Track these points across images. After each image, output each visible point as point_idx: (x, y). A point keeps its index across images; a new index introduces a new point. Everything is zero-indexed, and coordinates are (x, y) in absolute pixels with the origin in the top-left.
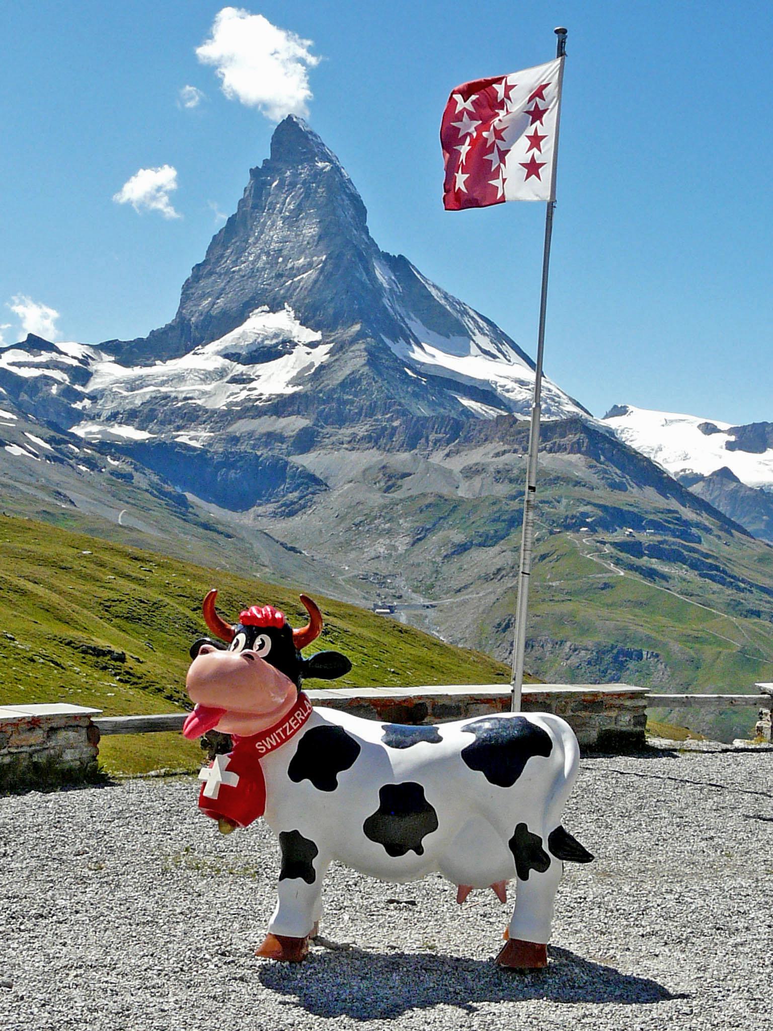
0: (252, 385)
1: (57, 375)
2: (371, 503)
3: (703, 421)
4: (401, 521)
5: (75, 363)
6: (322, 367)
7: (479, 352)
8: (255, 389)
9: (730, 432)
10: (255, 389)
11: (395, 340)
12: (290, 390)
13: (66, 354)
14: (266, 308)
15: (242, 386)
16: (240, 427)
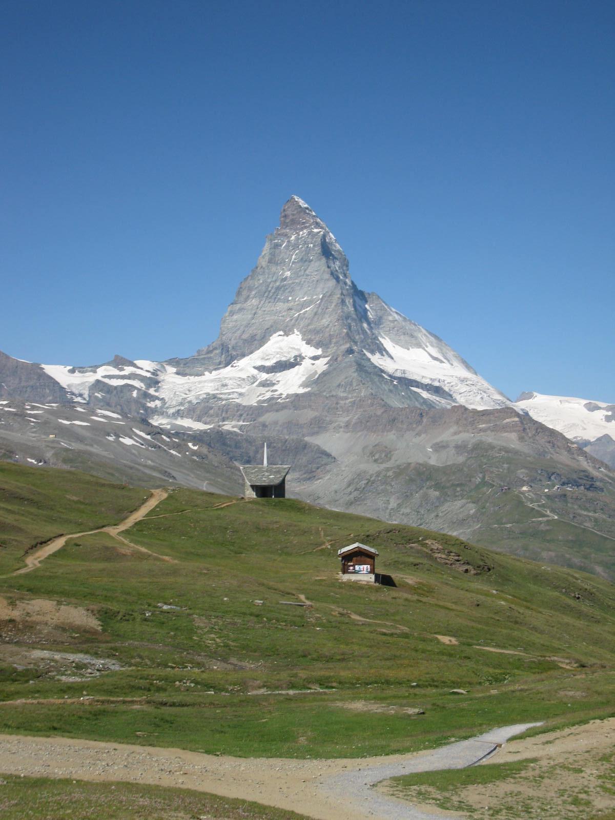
0: (275, 388)
1: (136, 383)
2: (371, 472)
3: (587, 401)
5: (149, 375)
6: (324, 374)
7: (430, 359)
8: (276, 391)
9: (607, 409)
10: (276, 391)
11: (373, 352)
12: (302, 391)
13: (142, 369)
14: (281, 333)
15: (267, 389)
16: (268, 418)
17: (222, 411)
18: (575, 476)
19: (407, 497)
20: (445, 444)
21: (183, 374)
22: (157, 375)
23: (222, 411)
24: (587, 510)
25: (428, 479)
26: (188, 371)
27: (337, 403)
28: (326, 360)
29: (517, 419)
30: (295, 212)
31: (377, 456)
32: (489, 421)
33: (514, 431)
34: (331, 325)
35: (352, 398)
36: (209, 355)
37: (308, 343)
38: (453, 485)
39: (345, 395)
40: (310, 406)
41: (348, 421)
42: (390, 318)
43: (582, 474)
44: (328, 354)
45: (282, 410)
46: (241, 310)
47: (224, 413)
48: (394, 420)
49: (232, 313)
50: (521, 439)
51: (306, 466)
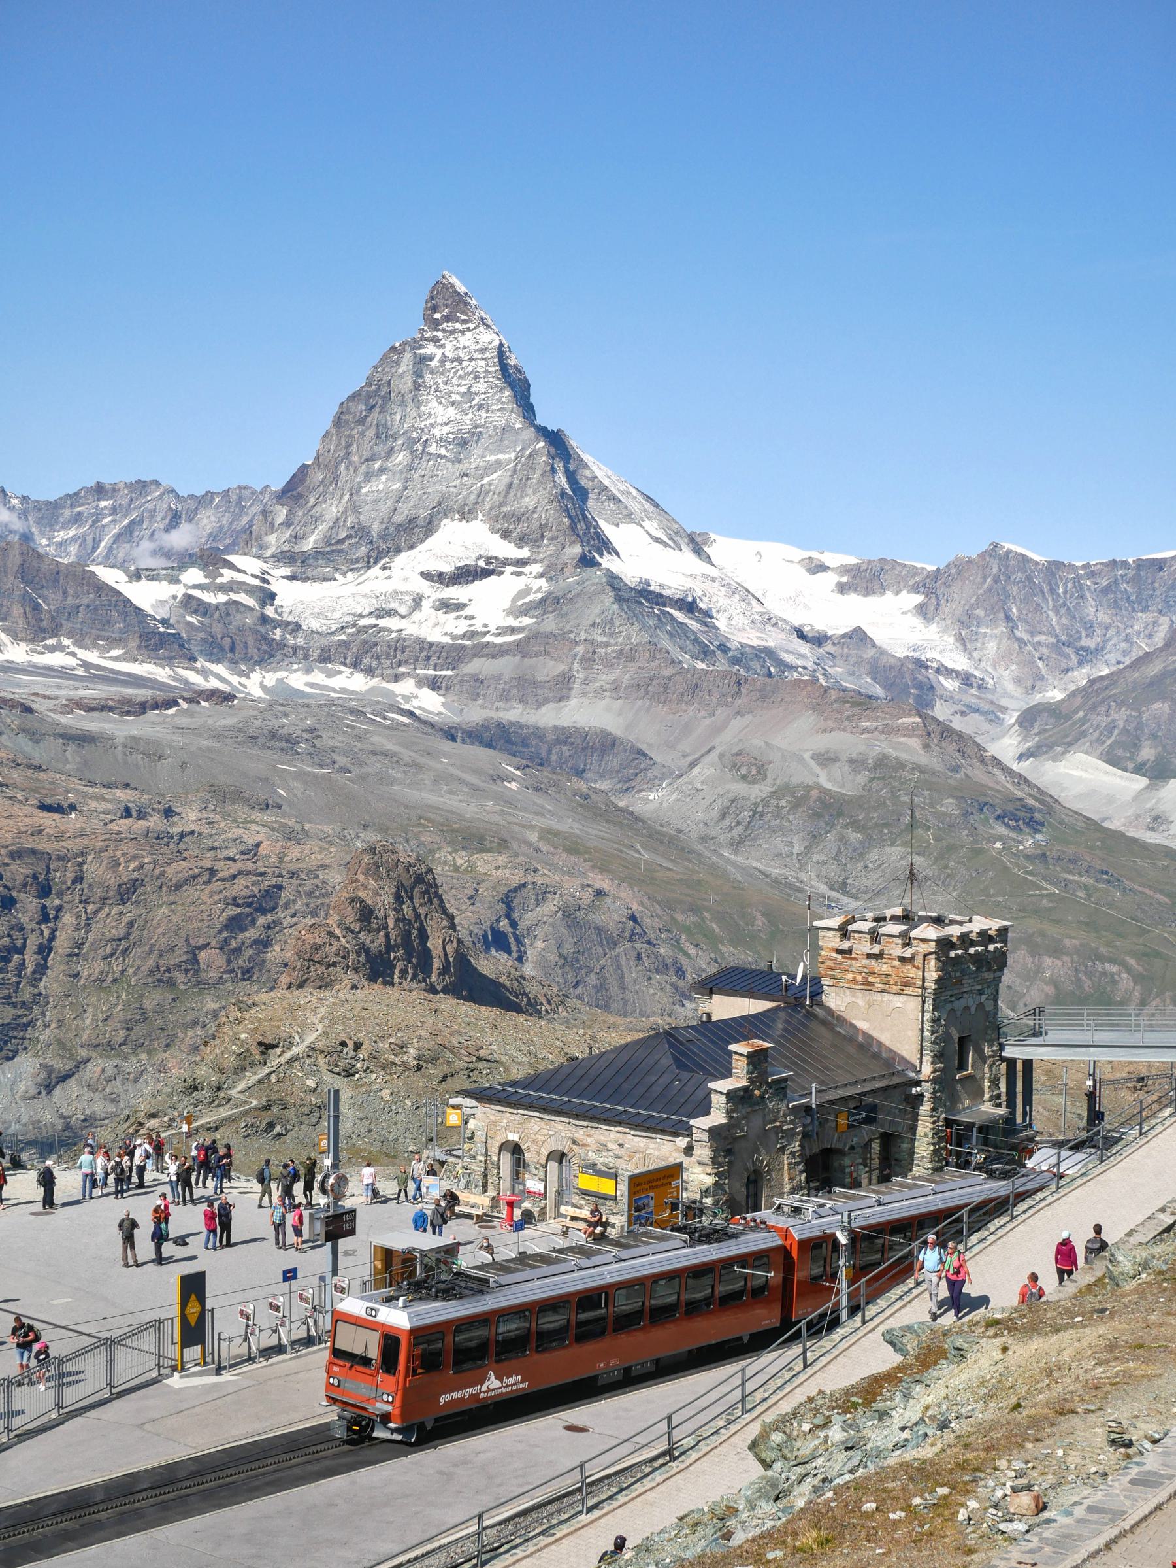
4: (791, 818)
5: (257, 582)
8: (472, 618)
13: (244, 572)
17: (395, 650)
18: (1010, 807)
19: (815, 839)
20: (833, 756)
21: (306, 579)
22: (268, 583)
23: (395, 650)
24: (1070, 872)
25: (839, 815)
26: (309, 573)
27: (594, 653)
28: (537, 568)
29: (918, 720)
30: (449, 302)
31: (744, 771)
32: (876, 719)
33: (917, 736)
34: (539, 509)
35: (616, 645)
36: (339, 547)
37: (505, 535)
38: (876, 824)
39: (605, 639)
40: (549, 654)
41: (614, 682)
42: (588, 473)
43: (1018, 803)
44: (541, 556)
45: (502, 656)
46: (382, 470)
47: (399, 653)
48: (696, 687)
49: (368, 477)
50: (926, 747)
51: (618, 772)
